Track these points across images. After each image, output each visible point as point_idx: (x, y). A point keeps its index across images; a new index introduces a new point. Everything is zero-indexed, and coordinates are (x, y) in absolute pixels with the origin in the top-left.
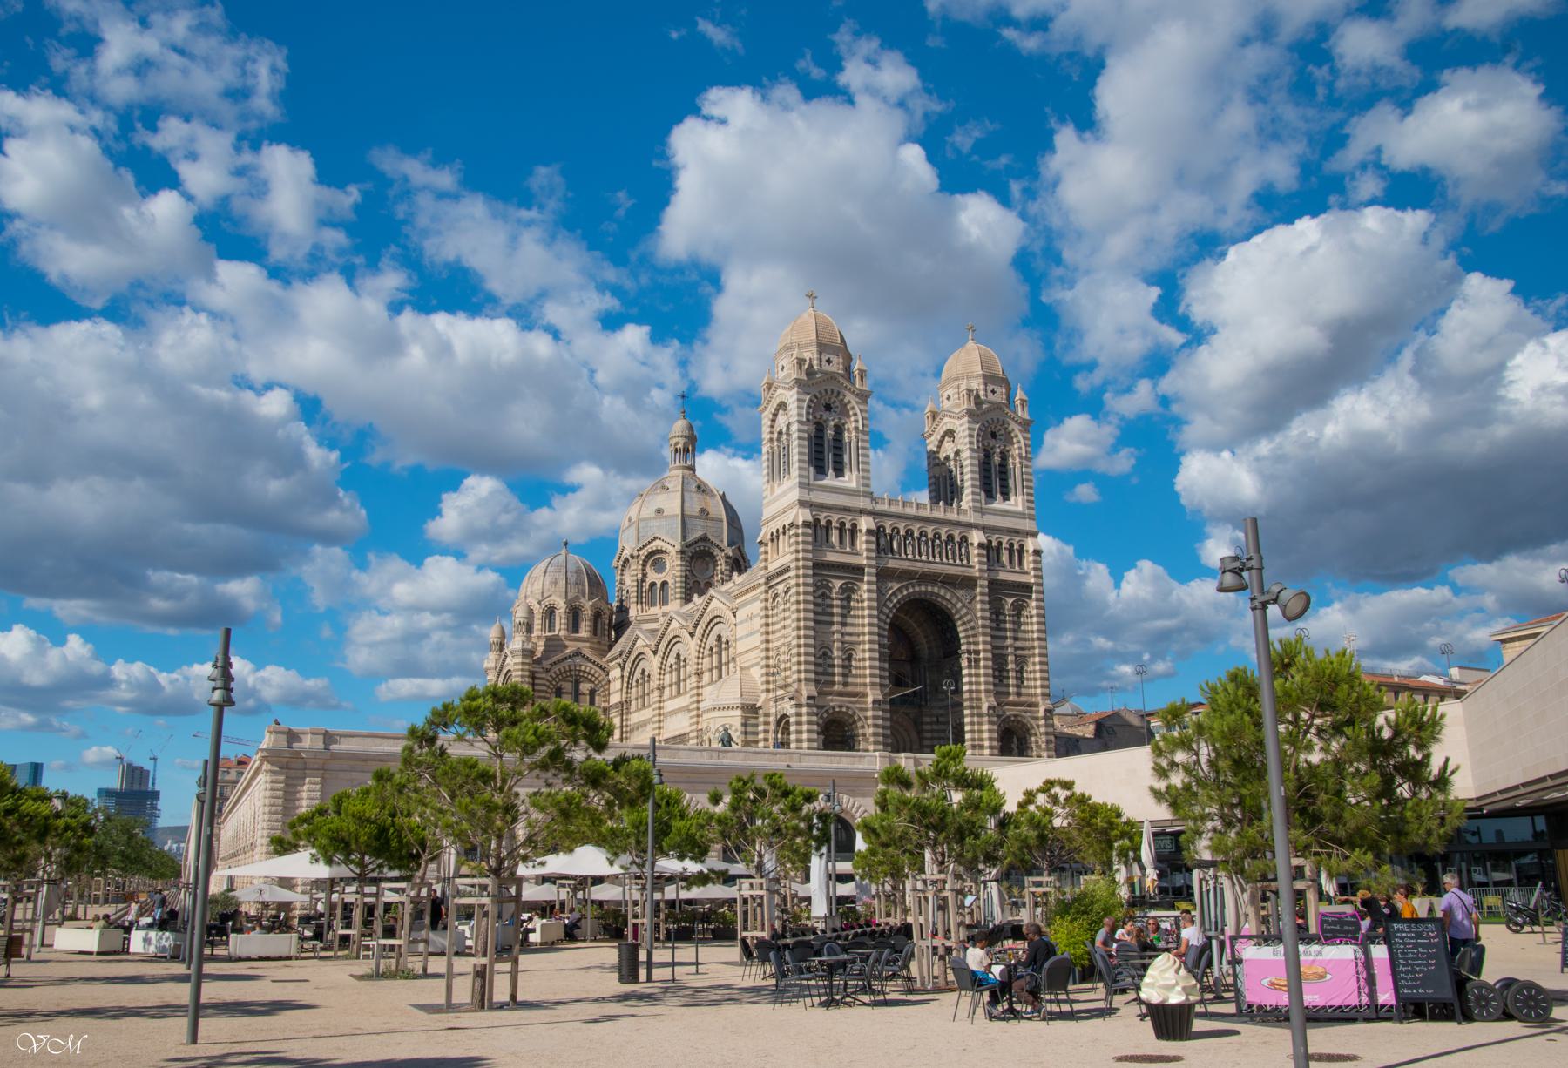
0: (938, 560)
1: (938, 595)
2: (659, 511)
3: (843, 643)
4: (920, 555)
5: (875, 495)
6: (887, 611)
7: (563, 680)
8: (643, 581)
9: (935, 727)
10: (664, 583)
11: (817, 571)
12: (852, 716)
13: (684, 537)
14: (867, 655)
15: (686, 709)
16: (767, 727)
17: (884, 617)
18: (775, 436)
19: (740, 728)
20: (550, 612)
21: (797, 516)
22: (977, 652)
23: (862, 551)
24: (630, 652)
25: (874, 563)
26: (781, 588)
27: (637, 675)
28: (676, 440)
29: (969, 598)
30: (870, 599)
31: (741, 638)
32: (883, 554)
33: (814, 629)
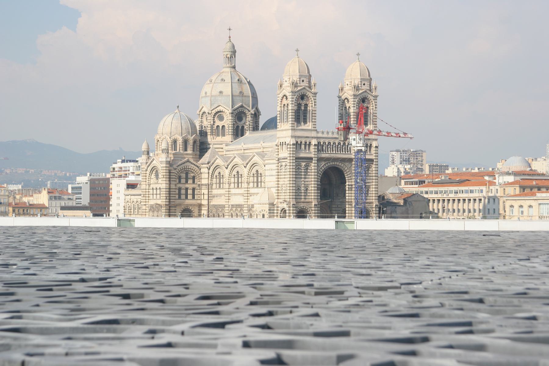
0: (339, 152)
1: (338, 165)
2: (221, 92)
3: (305, 184)
4: (333, 151)
5: (318, 130)
6: (320, 172)
7: (182, 173)
8: (213, 125)
9: (336, 209)
10: (223, 126)
11: (297, 160)
12: (307, 210)
13: (232, 107)
14: (313, 189)
15: (242, 195)
16: (277, 211)
17: (319, 175)
18: (282, 106)
19: (268, 211)
20: (175, 142)
21: (290, 141)
22: (352, 185)
23: (312, 152)
24: (213, 164)
25: (316, 156)
26: (284, 164)
27: (216, 173)
28: (227, 53)
29: (350, 166)
30: (314, 169)
31: (267, 176)
32: (320, 152)
33: (295, 181)
